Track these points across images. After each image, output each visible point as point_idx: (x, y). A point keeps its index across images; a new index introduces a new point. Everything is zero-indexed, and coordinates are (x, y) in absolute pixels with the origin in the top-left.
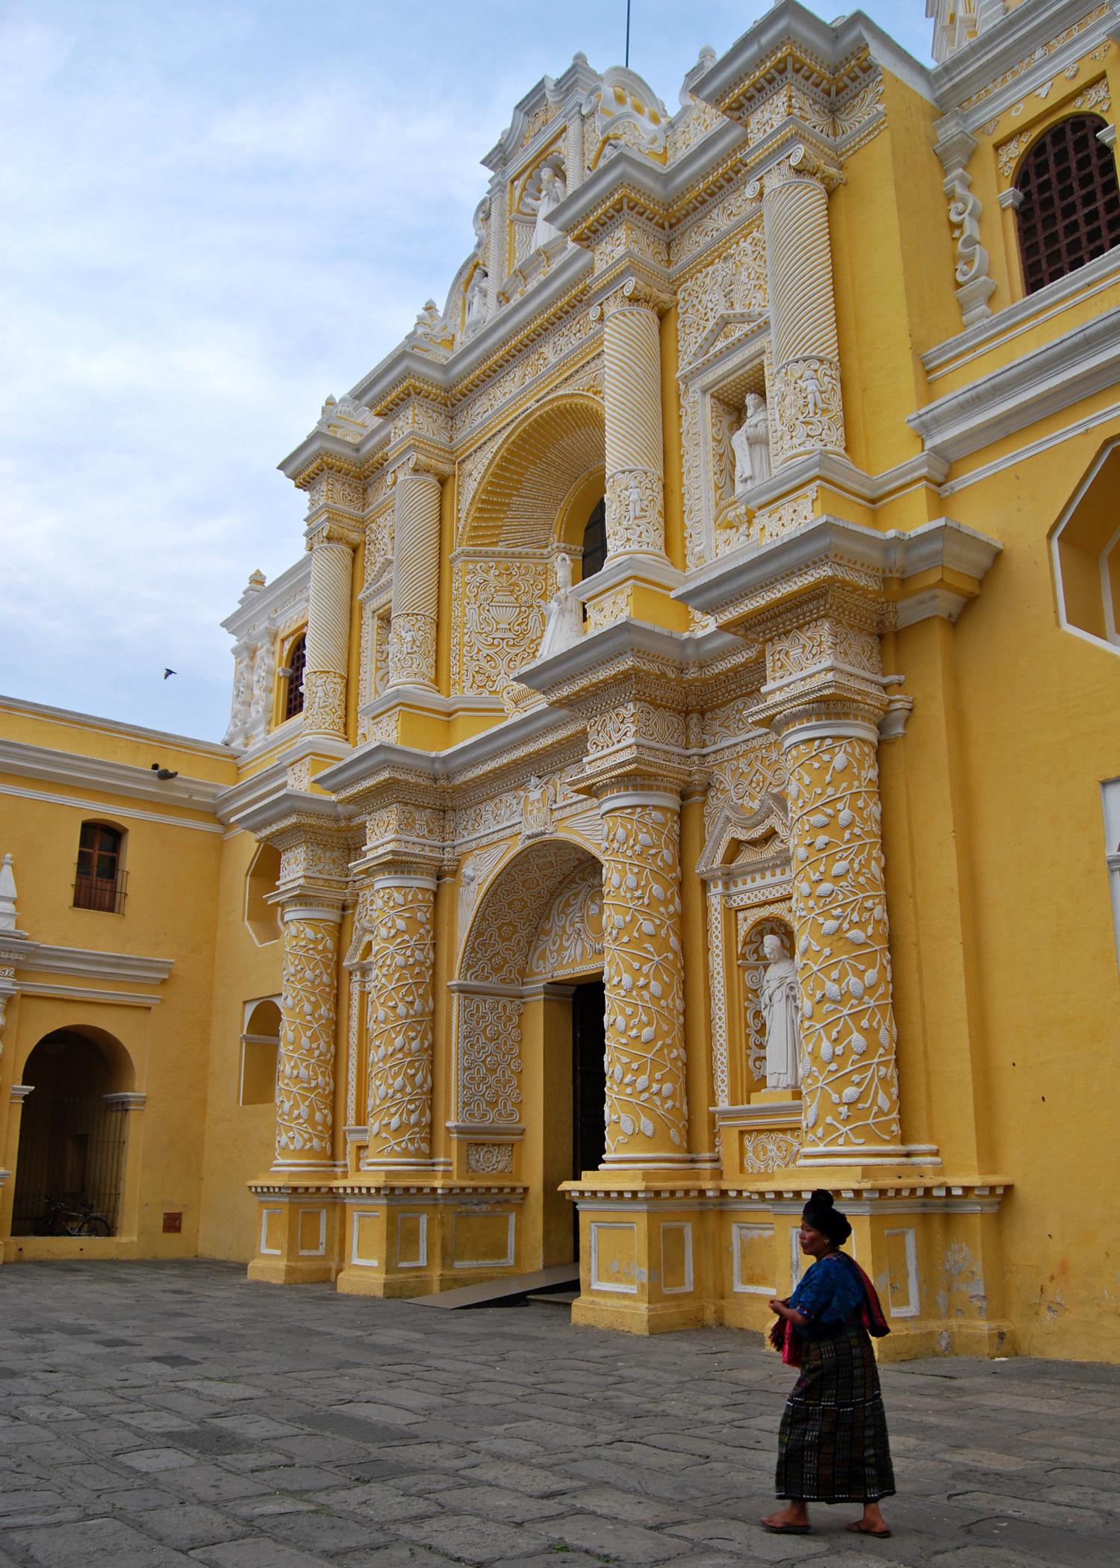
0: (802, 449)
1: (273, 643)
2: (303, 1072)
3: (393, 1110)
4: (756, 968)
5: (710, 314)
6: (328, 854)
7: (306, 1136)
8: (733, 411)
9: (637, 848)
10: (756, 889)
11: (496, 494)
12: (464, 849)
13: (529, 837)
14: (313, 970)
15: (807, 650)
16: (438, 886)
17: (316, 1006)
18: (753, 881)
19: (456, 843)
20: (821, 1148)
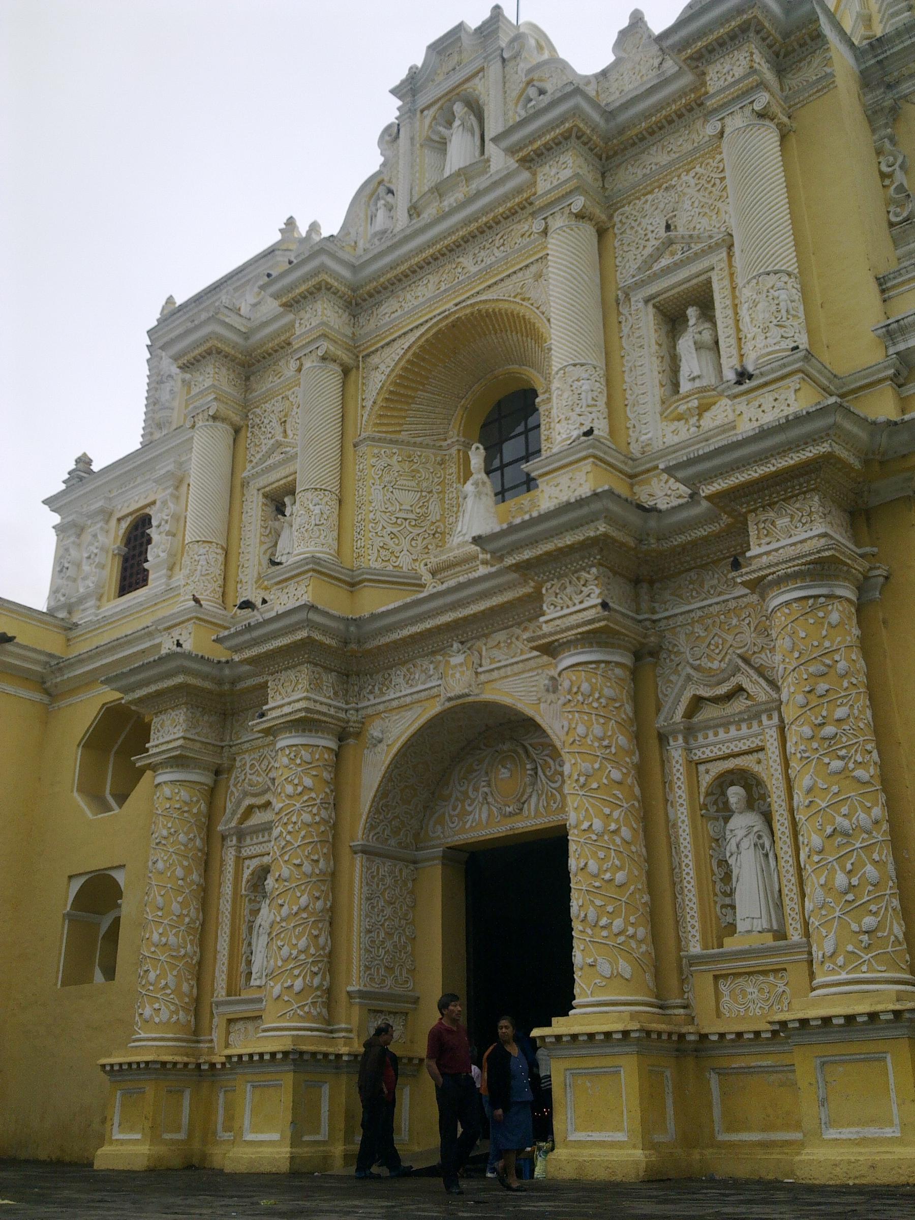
0: (777, 348)
1: (107, 522)
2: (172, 940)
3: (296, 972)
4: (717, 819)
5: (650, 235)
6: (206, 718)
7: (172, 1008)
8: (672, 320)
9: (602, 700)
10: (719, 743)
11: (406, 387)
12: (370, 711)
13: (450, 699)
14: (186, 834)
15: (797, 518)
16: (339, 747)
17: (188, 870)
18: (716, 735)
19: (360, 706)
20: (844, 976)
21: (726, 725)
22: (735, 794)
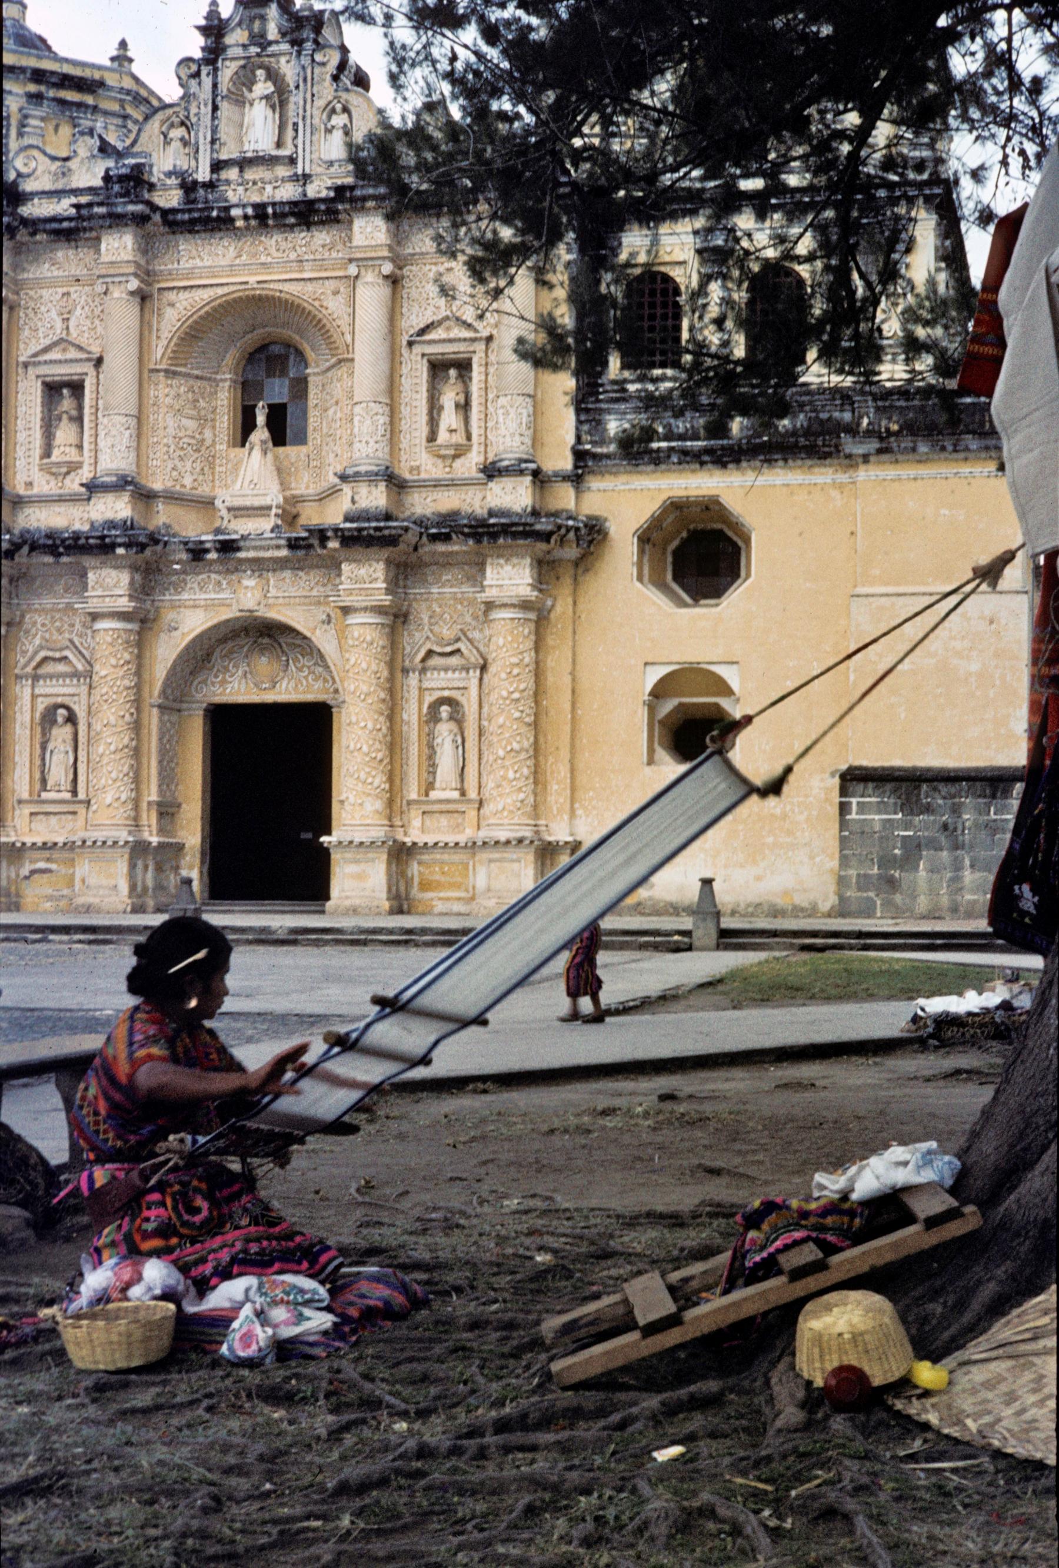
21: (446, 669)
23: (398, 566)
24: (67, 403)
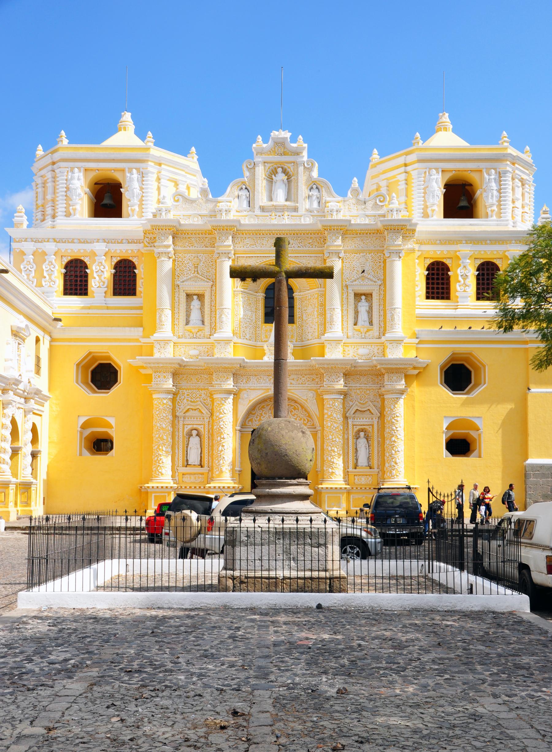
22: (362, 434)
23: (346, 375)
24: (195, 303)
